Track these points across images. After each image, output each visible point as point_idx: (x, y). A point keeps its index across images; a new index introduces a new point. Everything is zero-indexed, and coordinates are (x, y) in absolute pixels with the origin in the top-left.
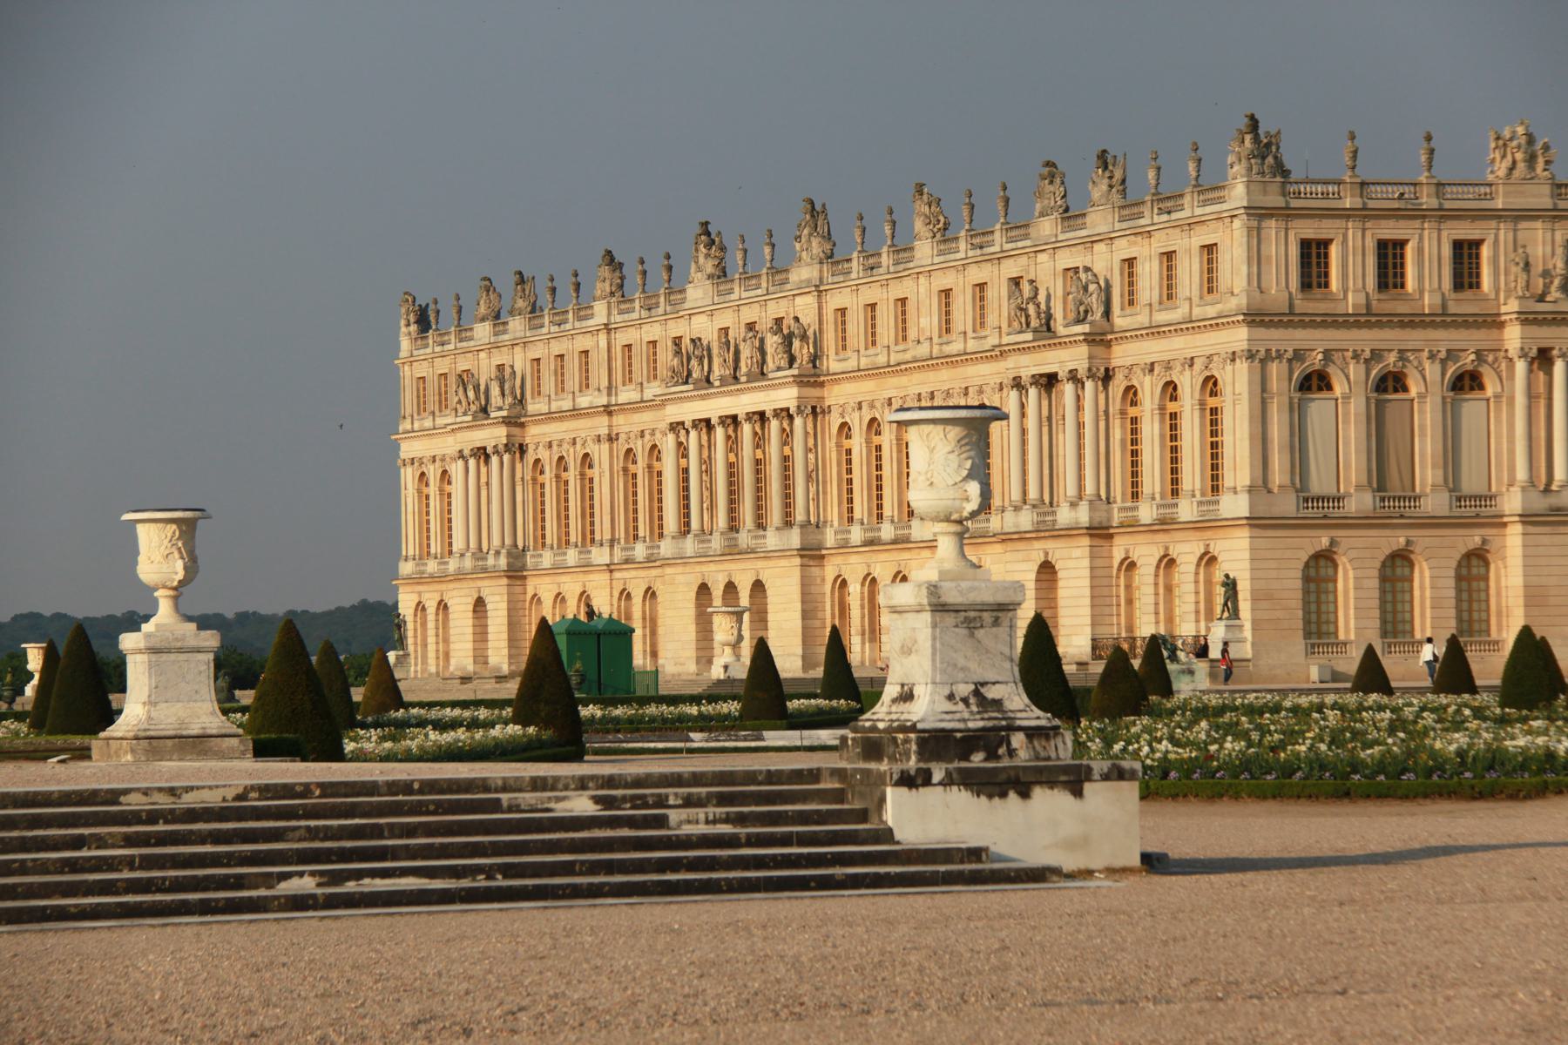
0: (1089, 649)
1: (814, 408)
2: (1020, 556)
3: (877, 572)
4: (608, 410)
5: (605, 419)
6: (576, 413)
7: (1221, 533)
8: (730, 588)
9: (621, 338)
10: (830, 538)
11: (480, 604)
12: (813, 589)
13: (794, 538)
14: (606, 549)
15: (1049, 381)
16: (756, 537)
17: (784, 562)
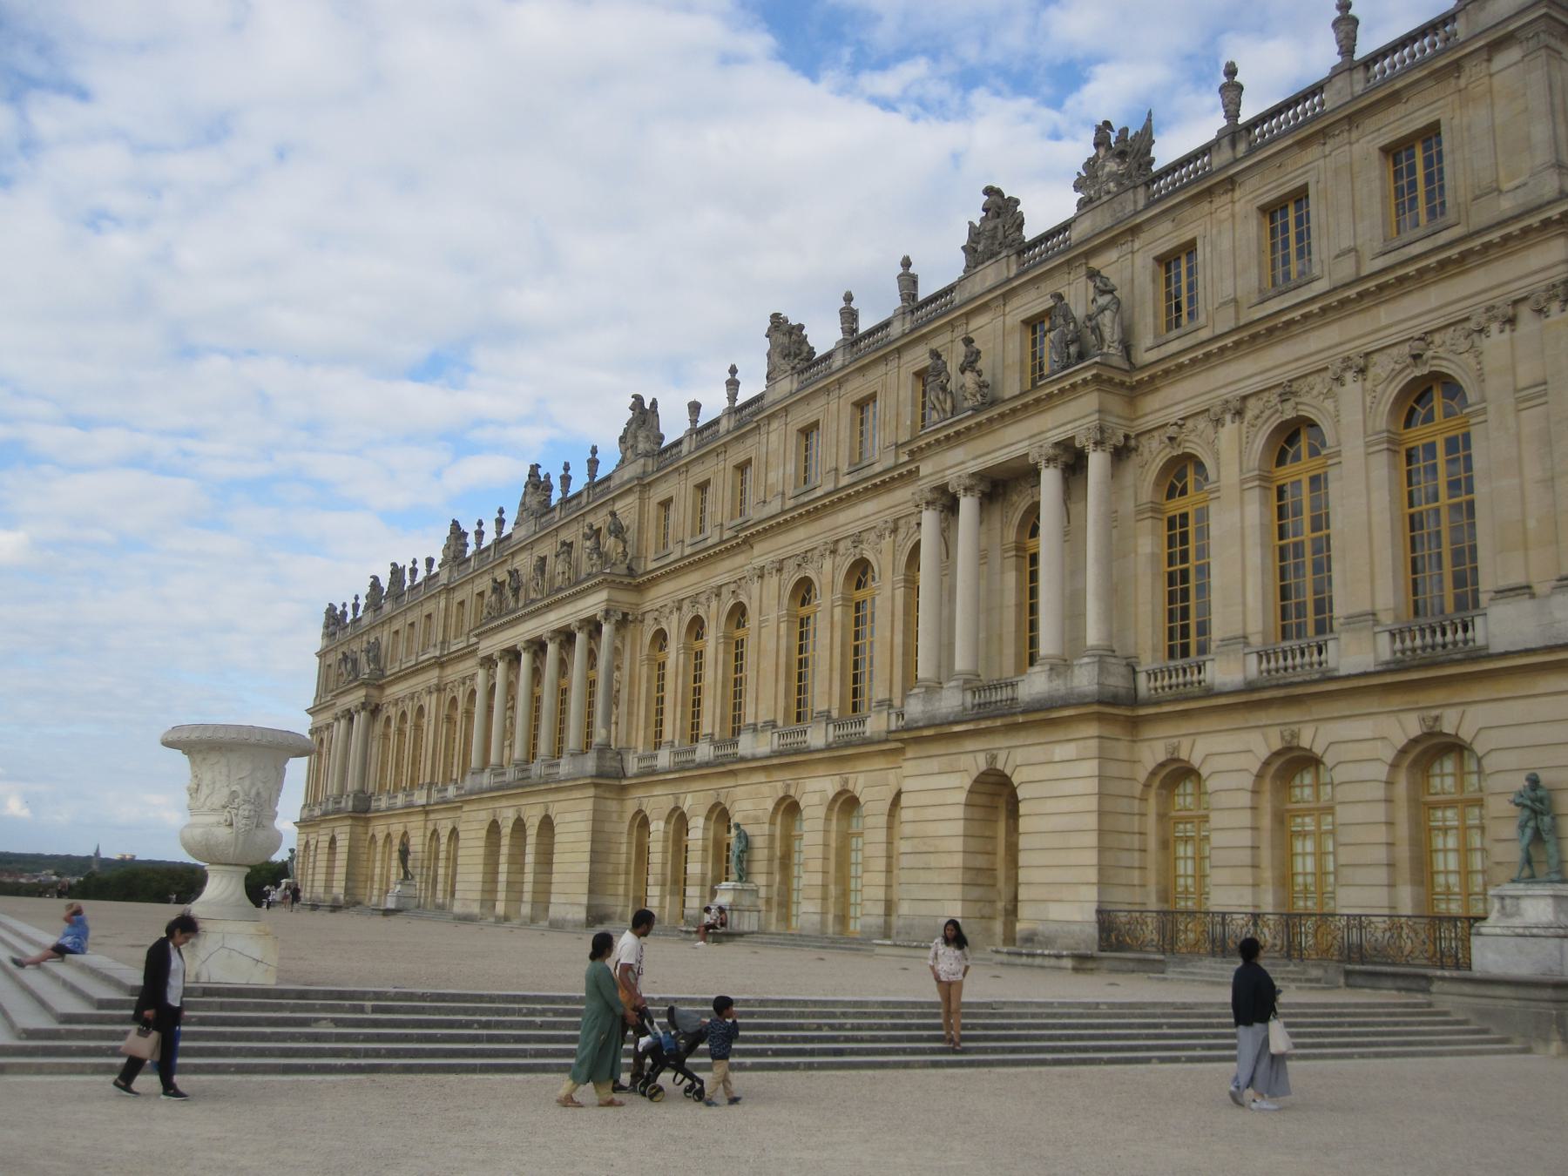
0: (1093, 931)
1: (625, 615)
2: (934, 765)
3: (687, 803)
4: (440, 663)
5: (436, 672)
6: (417, 670)
7: (1479, 692)
8: (519, 826)
9: (458, 596)
10: (633, 766)
11: (333, 841)
12: (608, 827)
13: (590, 764)
14: (425, 792)
15: (1000, 486)
16: (551, 766)
17: (576, 794)
